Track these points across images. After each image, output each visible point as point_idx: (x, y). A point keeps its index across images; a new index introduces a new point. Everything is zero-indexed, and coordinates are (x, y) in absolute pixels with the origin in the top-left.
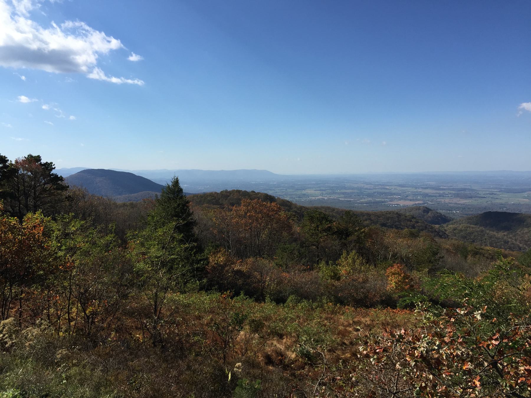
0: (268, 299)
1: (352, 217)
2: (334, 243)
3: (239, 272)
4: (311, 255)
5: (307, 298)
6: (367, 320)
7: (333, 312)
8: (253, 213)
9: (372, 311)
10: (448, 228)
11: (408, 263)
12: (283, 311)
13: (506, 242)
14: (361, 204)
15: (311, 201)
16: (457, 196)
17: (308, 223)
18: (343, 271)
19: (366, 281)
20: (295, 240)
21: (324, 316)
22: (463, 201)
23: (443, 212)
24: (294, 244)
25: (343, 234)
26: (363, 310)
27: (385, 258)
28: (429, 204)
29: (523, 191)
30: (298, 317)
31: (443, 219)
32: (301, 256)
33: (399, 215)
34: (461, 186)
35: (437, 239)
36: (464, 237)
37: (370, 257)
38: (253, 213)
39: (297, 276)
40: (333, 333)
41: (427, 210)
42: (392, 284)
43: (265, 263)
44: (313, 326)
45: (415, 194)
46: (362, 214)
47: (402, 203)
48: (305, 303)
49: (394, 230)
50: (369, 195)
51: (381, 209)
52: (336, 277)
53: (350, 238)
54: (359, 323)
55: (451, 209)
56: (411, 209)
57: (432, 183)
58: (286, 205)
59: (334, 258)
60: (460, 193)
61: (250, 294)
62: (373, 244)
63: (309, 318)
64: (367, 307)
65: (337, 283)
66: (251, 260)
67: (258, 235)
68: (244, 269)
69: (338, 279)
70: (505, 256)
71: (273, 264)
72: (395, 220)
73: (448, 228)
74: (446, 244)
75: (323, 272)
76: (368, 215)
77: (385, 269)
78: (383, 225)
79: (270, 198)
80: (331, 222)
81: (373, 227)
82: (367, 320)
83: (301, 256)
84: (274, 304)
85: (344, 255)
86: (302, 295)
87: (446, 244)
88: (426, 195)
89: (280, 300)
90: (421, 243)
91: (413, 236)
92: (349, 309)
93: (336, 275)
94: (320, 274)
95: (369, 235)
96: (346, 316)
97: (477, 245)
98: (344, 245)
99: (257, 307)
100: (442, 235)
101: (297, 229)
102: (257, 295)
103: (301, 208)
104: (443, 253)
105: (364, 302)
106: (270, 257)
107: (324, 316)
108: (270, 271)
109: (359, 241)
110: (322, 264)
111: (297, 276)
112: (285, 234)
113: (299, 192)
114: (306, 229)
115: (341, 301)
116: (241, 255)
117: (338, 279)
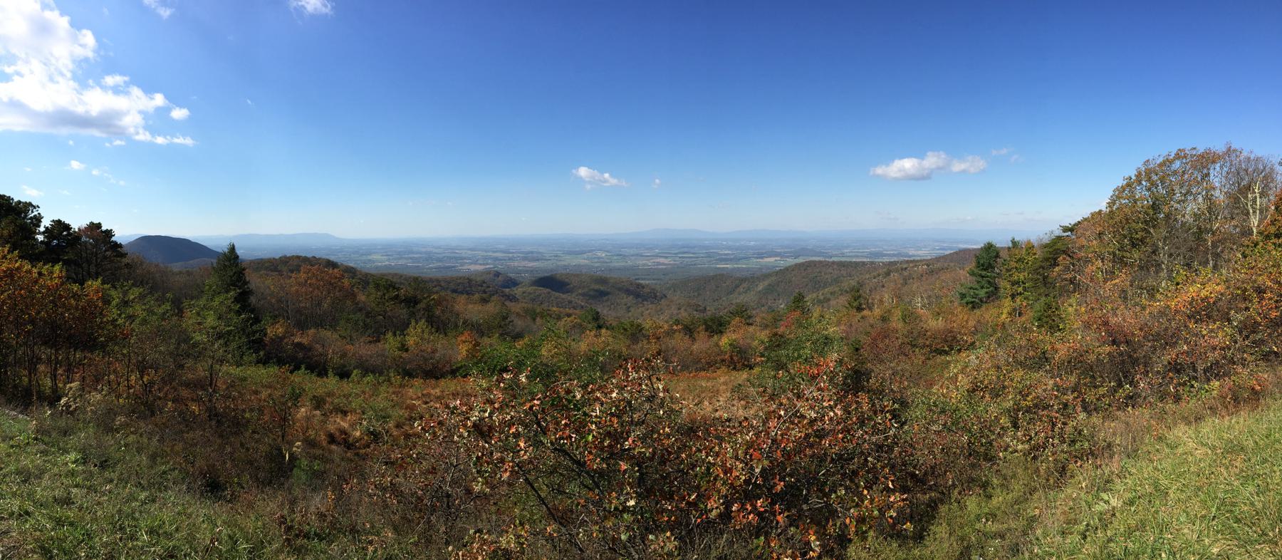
0: (330, 373)
1: (419, 283)
2: (403, 312)
3: (299, 345)
4: (376, 327)
5: (373, 372)
6: (437, 391)
7: (401, 386)
8: (314, 281)
9: (442, 382)
10: (518, 291)
11: (480, 330)
12: (347, 386)
13: (570, 302)
14: (429, 270)
15: (377, 267)
16: (525, 259)
17: (373, 291)
18: (411, 341)
19: (434, 351)
20: (360, 310)
21: (391, 390)
22: (531, 264)
23: (512, 275)
24: (358, 315)
25: (411, 302)
26: (433, 381)
27: (456, 326)
28: (500, 267)
29: (582, 253)
30: (364, 392)
31: (513, 283)
32: (366, 326)
33: (470, 280)
34: (529, 249)
35: (507, 303)
36: (533, 300)
37: (440, 325)
38: (314, 281)
39: (363, 349)
40: (401, 408)
41: (497, 274)
42: (463, 350)
43: (327, 334)
44: (381, 402)
45: (485, 258)
46: (431, 280)
47: (473, 268)
48: (370, 378)
49: (464, 297)
50: (439, 260)
51: (449, 274)
52: (404, 348)
53: (419, 306)
54: (429, 395)
55: (519, 272)
56: (482, 273)
57: (502, 247)
58: (351, 271)
59: (402, 328)
60: (528, 256)
61: (311, 368)
62: (443, 311)
63: (375, 393)
64: (437, 378)
65: (404, 355)
66: (312, 331)
67: (319, 304)
68: (305, 341)
69: (407, 350)
70: (569, 315)
71: (336, 336)
72: (468, 286)
73: (518, 291)
74: (515, 307)
75: (390, 343)
76: (438, 280)
77: (456, 337)
78: (454, 291)
79: (333, 265)
80: (398, 289)
81: (443, 294)
82: (437, 391)
83: (366, 326)
84: (337, 378)
85: (413, 323)
86: (367, 369)
87: (515, 307)
88: (496, 259)
89: (344, 374)
90: (492, 308)
91: (484, 301)
92: (418, 382)
93: (403, 345)
94: (387, 346)
95: (438, 303)
96: (415, 390)
97: (545, 306)
98: (413, 315)
99: (320, 382)
100: (512, 298)
101: (362, 297)
102: (319, 369)
103: (367, 274)
104: (512, 317)
105: (434, 373)
106: (333, 328)
107: (391, 390)
108: (331, 343)
109: (428, 309)
110: (389, 335)
111: (363, 349)
112: (349, 303)
113: (364, 258)
114: (372, 297)
115: (409, 374)
116: (302, 326)
117: (407, 350)
